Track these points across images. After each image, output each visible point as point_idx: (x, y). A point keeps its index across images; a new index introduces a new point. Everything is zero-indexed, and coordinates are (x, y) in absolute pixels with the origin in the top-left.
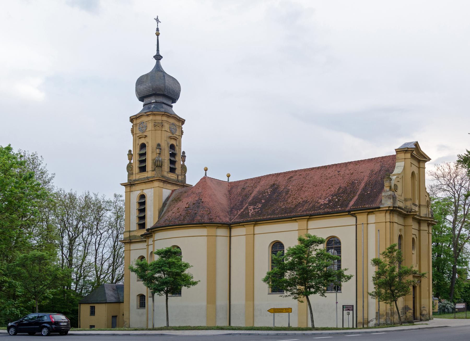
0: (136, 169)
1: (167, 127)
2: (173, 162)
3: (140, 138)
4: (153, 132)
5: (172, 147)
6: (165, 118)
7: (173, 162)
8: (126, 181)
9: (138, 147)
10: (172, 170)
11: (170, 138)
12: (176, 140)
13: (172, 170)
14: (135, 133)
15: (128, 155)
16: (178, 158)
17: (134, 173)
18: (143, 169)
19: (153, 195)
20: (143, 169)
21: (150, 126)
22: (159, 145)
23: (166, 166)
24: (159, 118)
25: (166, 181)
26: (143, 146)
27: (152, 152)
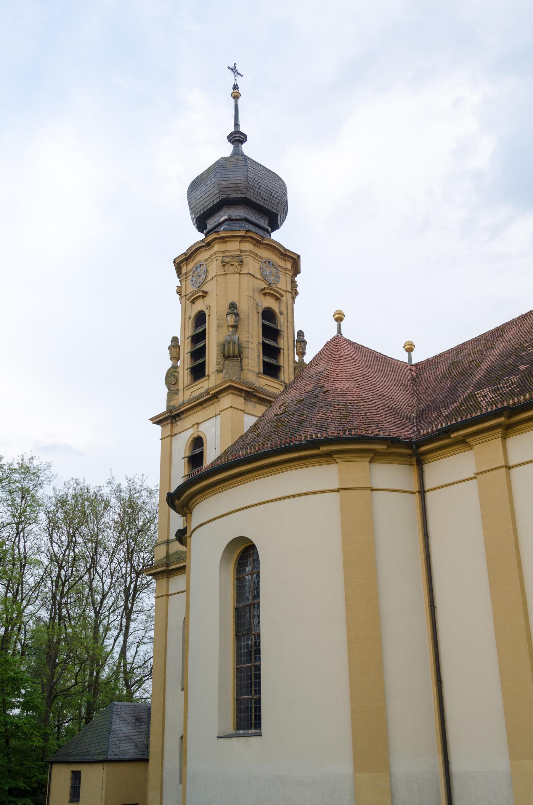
0: (184, 376)
1: (252, 266)
2: (271, 351)
3: (193, 302)
4: (220, 279)
5: (268, 315)
6: (247, 246)
7: (271, 351)
8: (161, 408)
9: (190, 324)
10: (271, 370)
11: (264, 293)
12: (277, 299)
13: (271, 370)
14: (183, 294)
15: (170, 348)
16: (284, 343)
17: (181, 387)
18: (198, 372)
19: (219, 432)
20: (198, 372)
21: (214, 268)
22: (233, 306)
23: (254, 359)
24: (233, 246)
25: (251, 395)
26: (200, 319)
27: (219, 326)
